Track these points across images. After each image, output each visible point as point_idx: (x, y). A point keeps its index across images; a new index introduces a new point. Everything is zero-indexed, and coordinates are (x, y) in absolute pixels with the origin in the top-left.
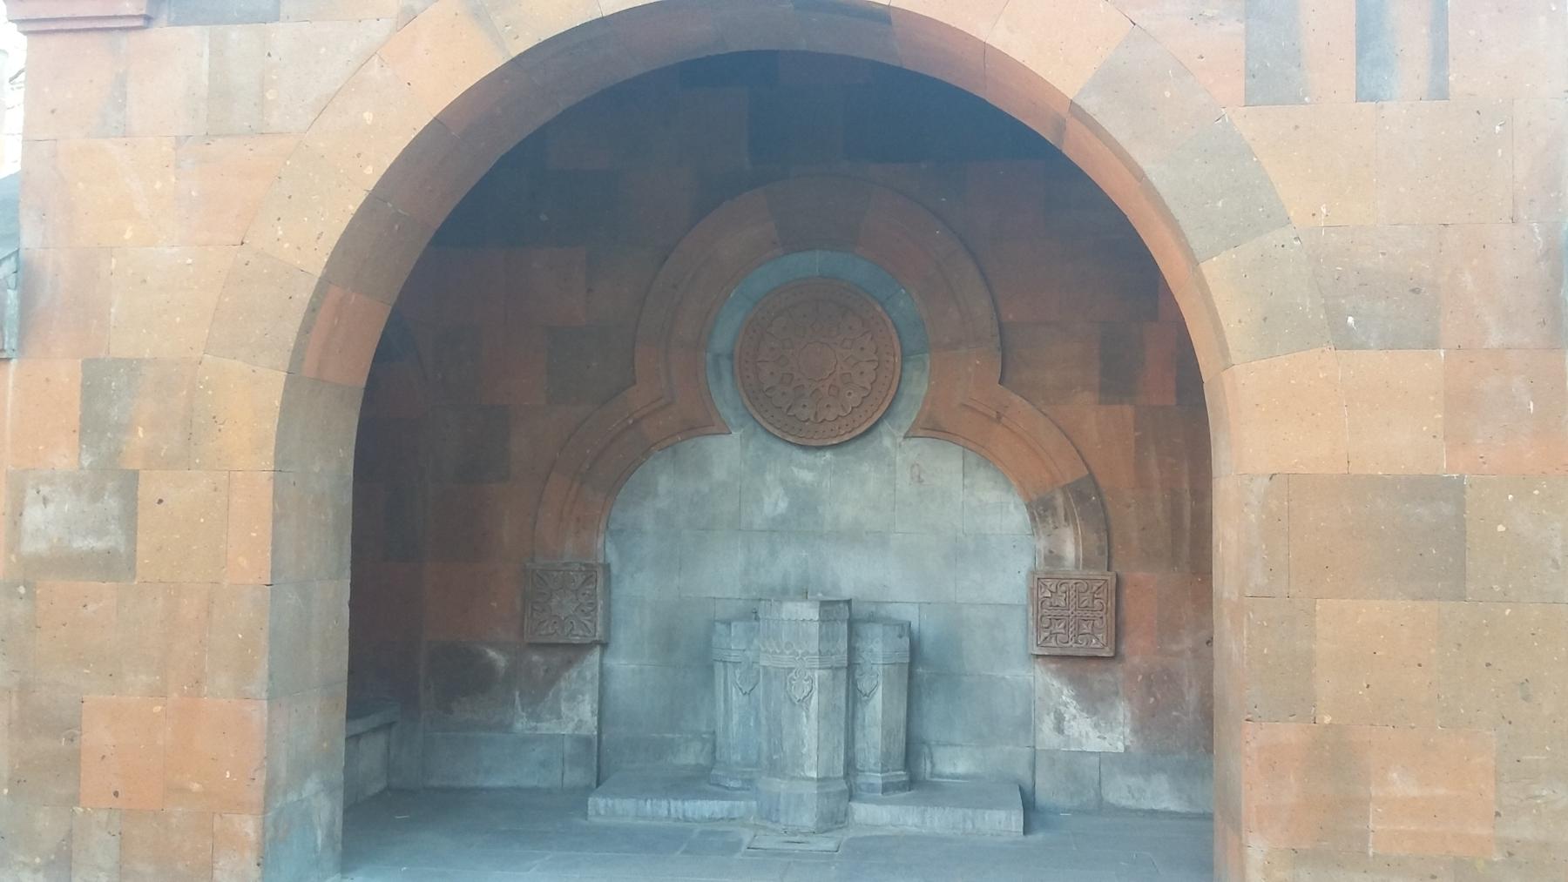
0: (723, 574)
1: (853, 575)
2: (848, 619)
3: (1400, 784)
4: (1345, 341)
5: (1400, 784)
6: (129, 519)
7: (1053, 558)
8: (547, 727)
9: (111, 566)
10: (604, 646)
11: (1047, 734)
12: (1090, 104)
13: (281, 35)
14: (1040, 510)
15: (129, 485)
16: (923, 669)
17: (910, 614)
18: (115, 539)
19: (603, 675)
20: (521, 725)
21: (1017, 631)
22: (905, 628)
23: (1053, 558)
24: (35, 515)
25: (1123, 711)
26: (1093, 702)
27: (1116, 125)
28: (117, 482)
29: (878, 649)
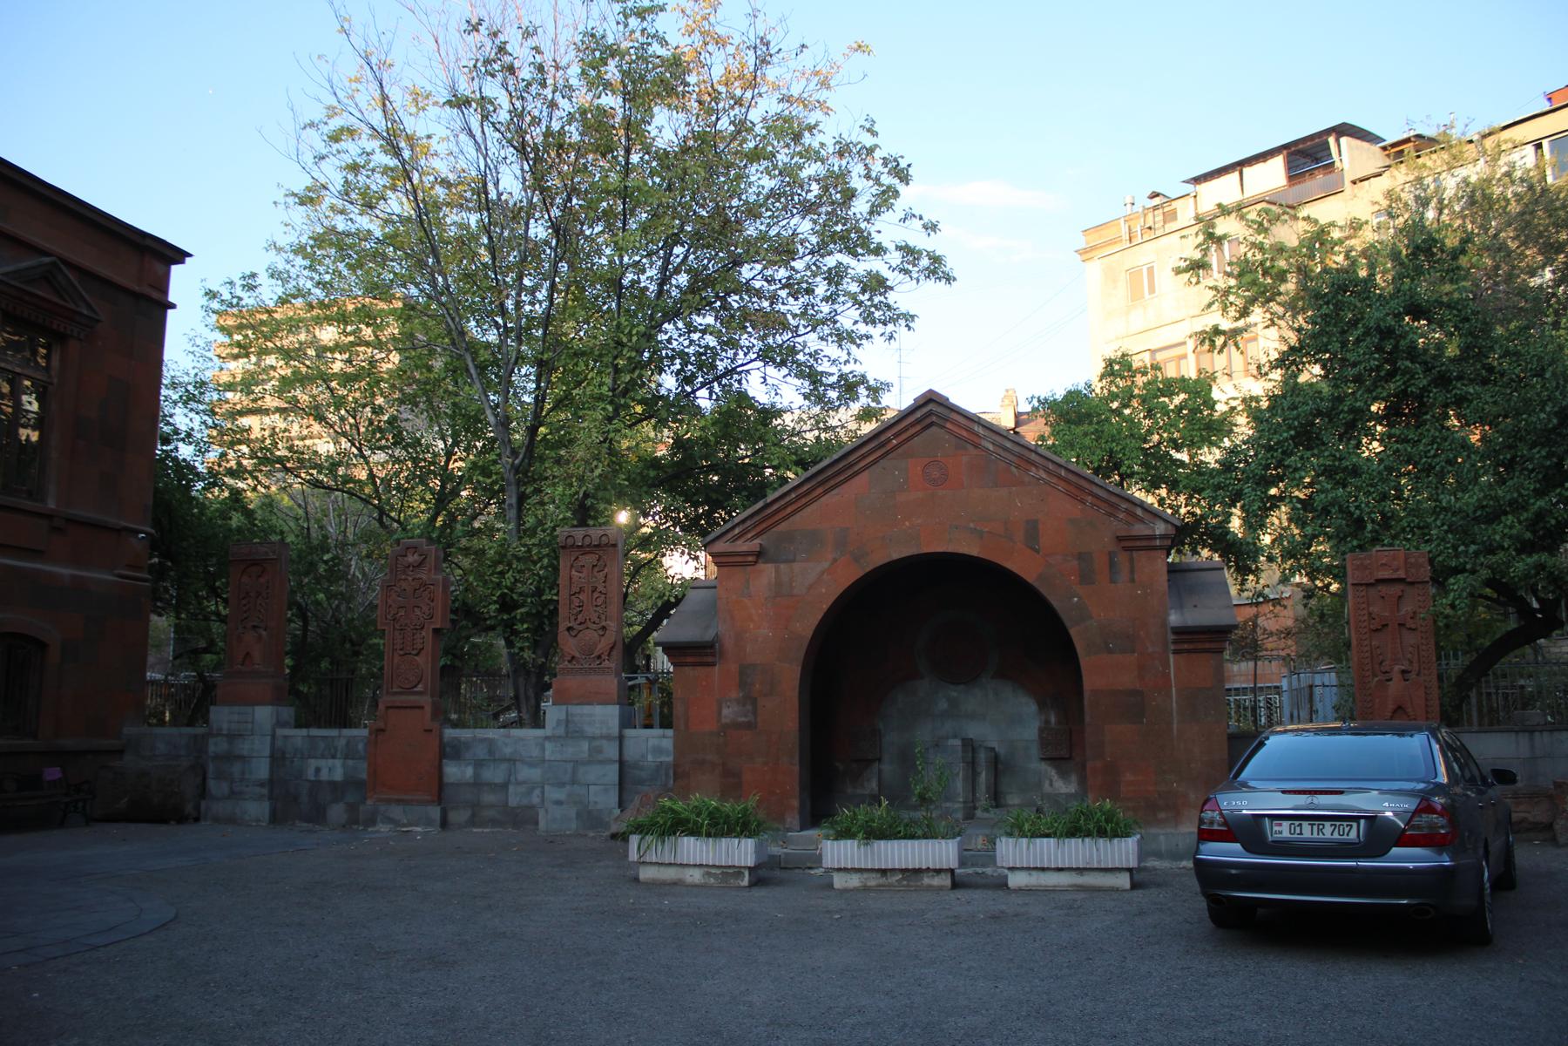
0: (923, 734)
1: (974, 730)
2: (970, 746)
3: (1129, 777)
4: (1110, 651)
5: (1129, 777)
6: (755, 713)
7: (1047, 722)
8: (859, 791)
9: (749, 726)
10: (880, 760)
11: (1046, 787)
12: (1036, 584)
13: (797, 566)
14: (1042, 705)
15: (754, 702)
16: (998, 765)
17: (995, 745)
18: (750, 718)
19: (880, 771)
20: (849, 790)
21: (1035, 751)
22: (993, 749)
23: (1047, 722)
24: (725, 711)
25: (1074, 778)
26: (1063, 775)
27: (1043, 591)
28: (750, 700)
29: (982, 756)
